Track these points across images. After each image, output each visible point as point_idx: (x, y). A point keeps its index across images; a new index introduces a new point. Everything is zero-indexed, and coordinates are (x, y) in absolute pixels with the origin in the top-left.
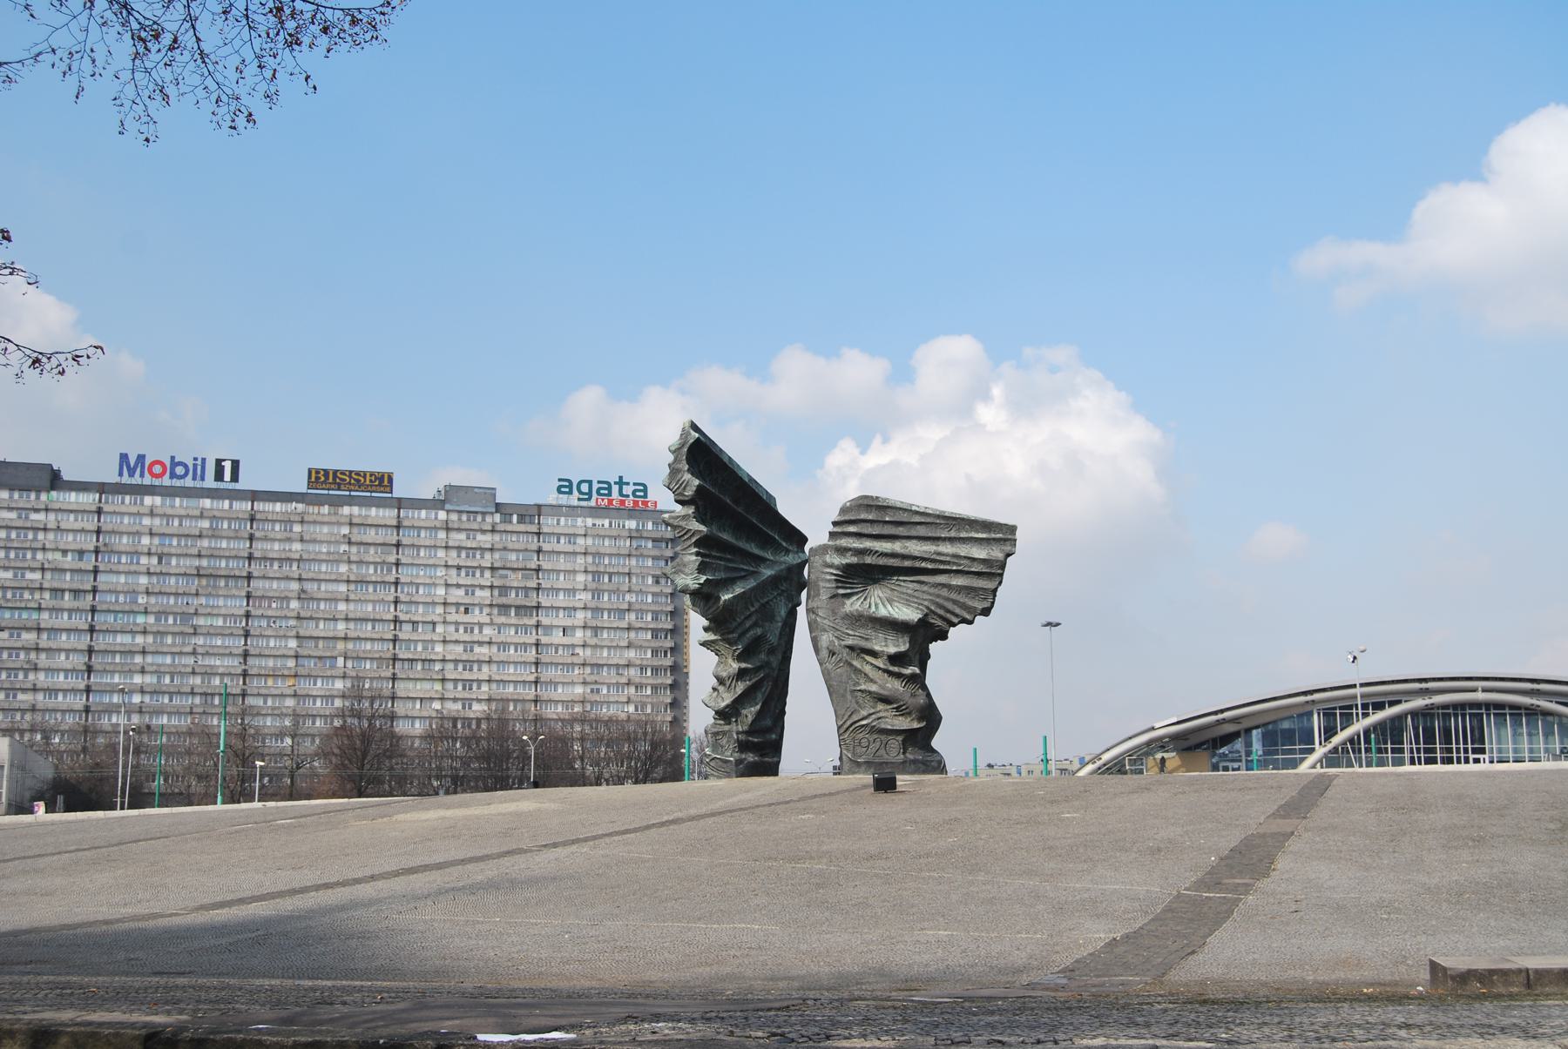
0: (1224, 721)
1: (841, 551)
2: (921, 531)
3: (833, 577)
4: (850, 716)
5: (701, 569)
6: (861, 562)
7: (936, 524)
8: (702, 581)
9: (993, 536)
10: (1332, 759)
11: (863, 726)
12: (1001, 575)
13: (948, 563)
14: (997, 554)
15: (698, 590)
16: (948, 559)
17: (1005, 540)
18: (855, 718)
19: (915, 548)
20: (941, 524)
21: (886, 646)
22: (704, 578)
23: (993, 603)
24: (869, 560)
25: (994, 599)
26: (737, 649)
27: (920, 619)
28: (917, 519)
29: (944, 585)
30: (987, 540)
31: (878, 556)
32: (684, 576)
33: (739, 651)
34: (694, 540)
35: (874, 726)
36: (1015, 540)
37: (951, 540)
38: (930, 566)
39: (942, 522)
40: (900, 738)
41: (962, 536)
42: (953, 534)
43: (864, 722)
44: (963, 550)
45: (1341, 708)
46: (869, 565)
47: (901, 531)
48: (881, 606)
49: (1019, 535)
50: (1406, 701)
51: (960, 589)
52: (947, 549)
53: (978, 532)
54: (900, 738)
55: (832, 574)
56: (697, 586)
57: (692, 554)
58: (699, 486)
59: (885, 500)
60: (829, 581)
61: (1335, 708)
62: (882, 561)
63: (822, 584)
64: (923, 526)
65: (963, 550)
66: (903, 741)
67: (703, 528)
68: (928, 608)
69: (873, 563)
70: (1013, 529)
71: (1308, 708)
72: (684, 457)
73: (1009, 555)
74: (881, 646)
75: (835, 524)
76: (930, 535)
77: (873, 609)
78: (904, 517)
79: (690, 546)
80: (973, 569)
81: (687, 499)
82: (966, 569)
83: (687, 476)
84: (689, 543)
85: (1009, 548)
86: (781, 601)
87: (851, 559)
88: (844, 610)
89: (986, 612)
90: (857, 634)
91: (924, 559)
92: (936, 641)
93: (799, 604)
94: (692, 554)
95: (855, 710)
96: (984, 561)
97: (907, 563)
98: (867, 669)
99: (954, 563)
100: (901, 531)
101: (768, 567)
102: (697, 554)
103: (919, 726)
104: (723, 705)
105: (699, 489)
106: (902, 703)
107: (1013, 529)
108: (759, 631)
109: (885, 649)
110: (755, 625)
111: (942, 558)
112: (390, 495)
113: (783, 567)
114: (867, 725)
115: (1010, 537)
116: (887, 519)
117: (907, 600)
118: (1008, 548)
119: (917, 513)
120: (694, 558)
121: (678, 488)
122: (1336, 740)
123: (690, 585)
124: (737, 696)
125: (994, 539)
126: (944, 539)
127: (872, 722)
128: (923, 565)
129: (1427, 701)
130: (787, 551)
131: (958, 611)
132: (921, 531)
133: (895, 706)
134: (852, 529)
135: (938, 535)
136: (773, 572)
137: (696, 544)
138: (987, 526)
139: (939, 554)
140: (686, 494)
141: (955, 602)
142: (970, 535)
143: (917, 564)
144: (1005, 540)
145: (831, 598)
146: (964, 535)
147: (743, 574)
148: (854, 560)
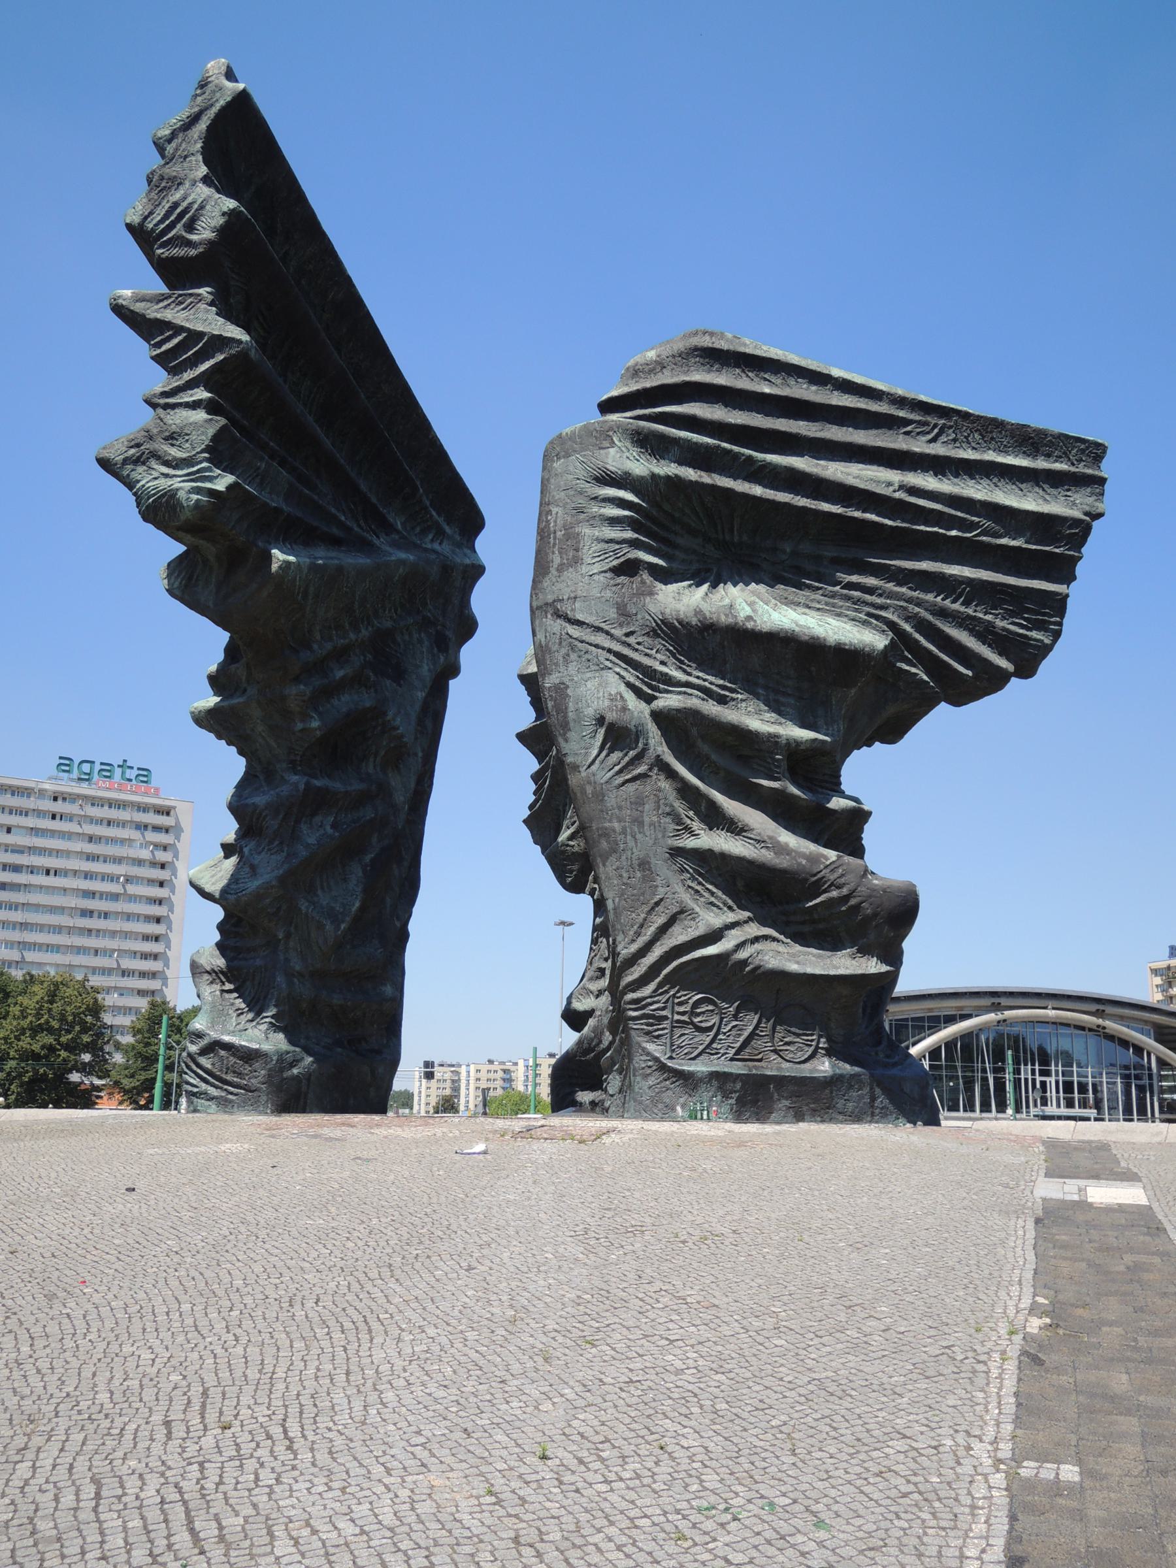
3: (627, 513)
4: (663, 930)
12: (1074, 561)
20: (910, 422)
22: (230, 479)
25: (1060, 624)
32: (165, 470)
35: (745, 962)
39: (912, 416)
42: (938, 449)
44: (977, 490)
50: (976, 1016)
55: (621, 503)
57: (194, 405)
58: (231, 214)
60: (613, 521)
61: (907, 1020)
63: (586, 531)
68: (892, 626)
70: (1096, 452)
72: (199, 145)
81: (193, 252)
84: (188, 375)
85: (1090, 500)
86: (420, 641)
87: (668, 469)
94: (194, 405)
95: (682, 912)
99: (952, 522)
101: (396, 545)
102: (212, 407)
105: (232, 225)
107: (1096, 452)
108: (367, 700)
110: (357, 681)
111: (922, 502)
115: (1081, 469)
117: (827, 604)
120: (201, 415)
123: (182, 495)
129: (1000, 1016)
130: (440, 534)
139: (914, 491)
140: (194, 237)
145: (617, 571)
147: (335, 531)
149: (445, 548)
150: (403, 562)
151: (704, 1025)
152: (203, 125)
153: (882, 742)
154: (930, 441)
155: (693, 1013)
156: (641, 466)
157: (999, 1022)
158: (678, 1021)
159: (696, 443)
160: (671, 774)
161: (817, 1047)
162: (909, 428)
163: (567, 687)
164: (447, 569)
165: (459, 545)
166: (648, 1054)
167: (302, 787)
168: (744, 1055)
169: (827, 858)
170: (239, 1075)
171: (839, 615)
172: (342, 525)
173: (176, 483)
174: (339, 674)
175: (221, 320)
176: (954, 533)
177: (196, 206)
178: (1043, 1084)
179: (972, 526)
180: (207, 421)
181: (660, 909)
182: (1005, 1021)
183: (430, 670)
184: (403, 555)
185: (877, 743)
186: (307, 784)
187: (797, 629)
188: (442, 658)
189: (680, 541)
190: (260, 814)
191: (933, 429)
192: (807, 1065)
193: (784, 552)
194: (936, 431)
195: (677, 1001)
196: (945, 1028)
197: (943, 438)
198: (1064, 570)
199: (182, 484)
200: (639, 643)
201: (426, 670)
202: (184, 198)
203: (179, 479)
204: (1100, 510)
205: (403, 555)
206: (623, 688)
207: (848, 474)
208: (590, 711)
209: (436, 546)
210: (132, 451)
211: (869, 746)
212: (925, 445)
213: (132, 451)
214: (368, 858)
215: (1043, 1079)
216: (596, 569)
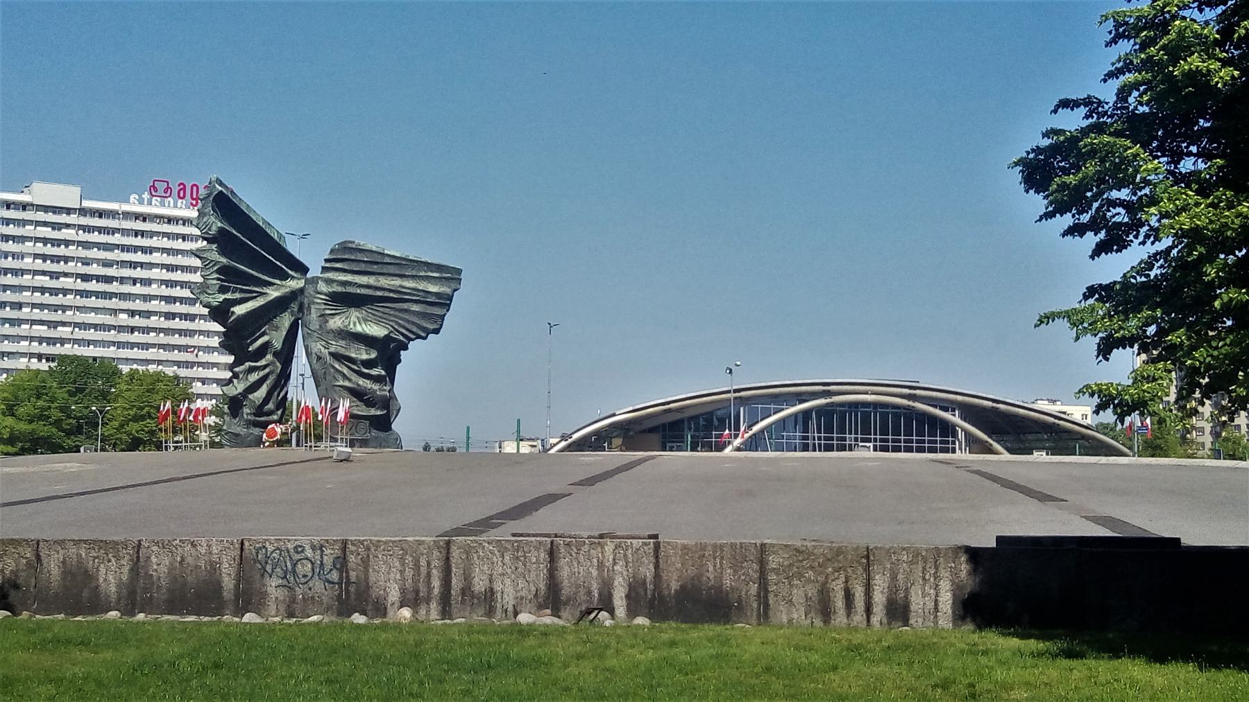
0: (670, 410)
1: (329, 282)
8: (221, 300)
10: (754, 444)
12: (449, 305)
14: (445, 289)
15: (216, 307)
16: (409, 291)
19: (384, 282)
23: (442, 325)
28: (387, 260)
34: (215, 268)
37: (413, 277)
41: (421, 274)
42: (414, 274)
44: (422, 286)
47: (375, 268)
48: (357, 324)
52: (410, 284)
53: (432, 272)
64: (392, 266)
65: (422, 286)
70: (459, 271)
73: (455, 290)
75: (327, 260)
76: (397, 272)
77: (352, 326)
81: (211, 236)
84: (212, 271)
85: (456, 285)
89: (437, 331)
91: (390, 291)
96: (437, 295)
97: (379, 293)
98: (345, 370)
99: (414, 295)
101: (276, 290)
103: (382, 413)
107: (459, 271)
109: (359, 356)
113: (288, 290)
115: (456, 276)
116: (366, 259)
118: (454, 286)
121: (205, 228)
122: (756, 428)
125: (445, 278)
128: (392, 295)
129: (829, 400)
130: (293, 278)
131: (415, 329)
132: (392, 270)
134: (338, 265)
137: (218, 271)
138: (439, 268)
141: (413, 323)
142: (427, 274)
143: (387, 294)
145: (320, 316)
147: (254, 295)
148: (340, 289)
160: (334, 367)
173: (210, 300)
179: (419, 296)
198: (447, 306)
206: (321, 347)
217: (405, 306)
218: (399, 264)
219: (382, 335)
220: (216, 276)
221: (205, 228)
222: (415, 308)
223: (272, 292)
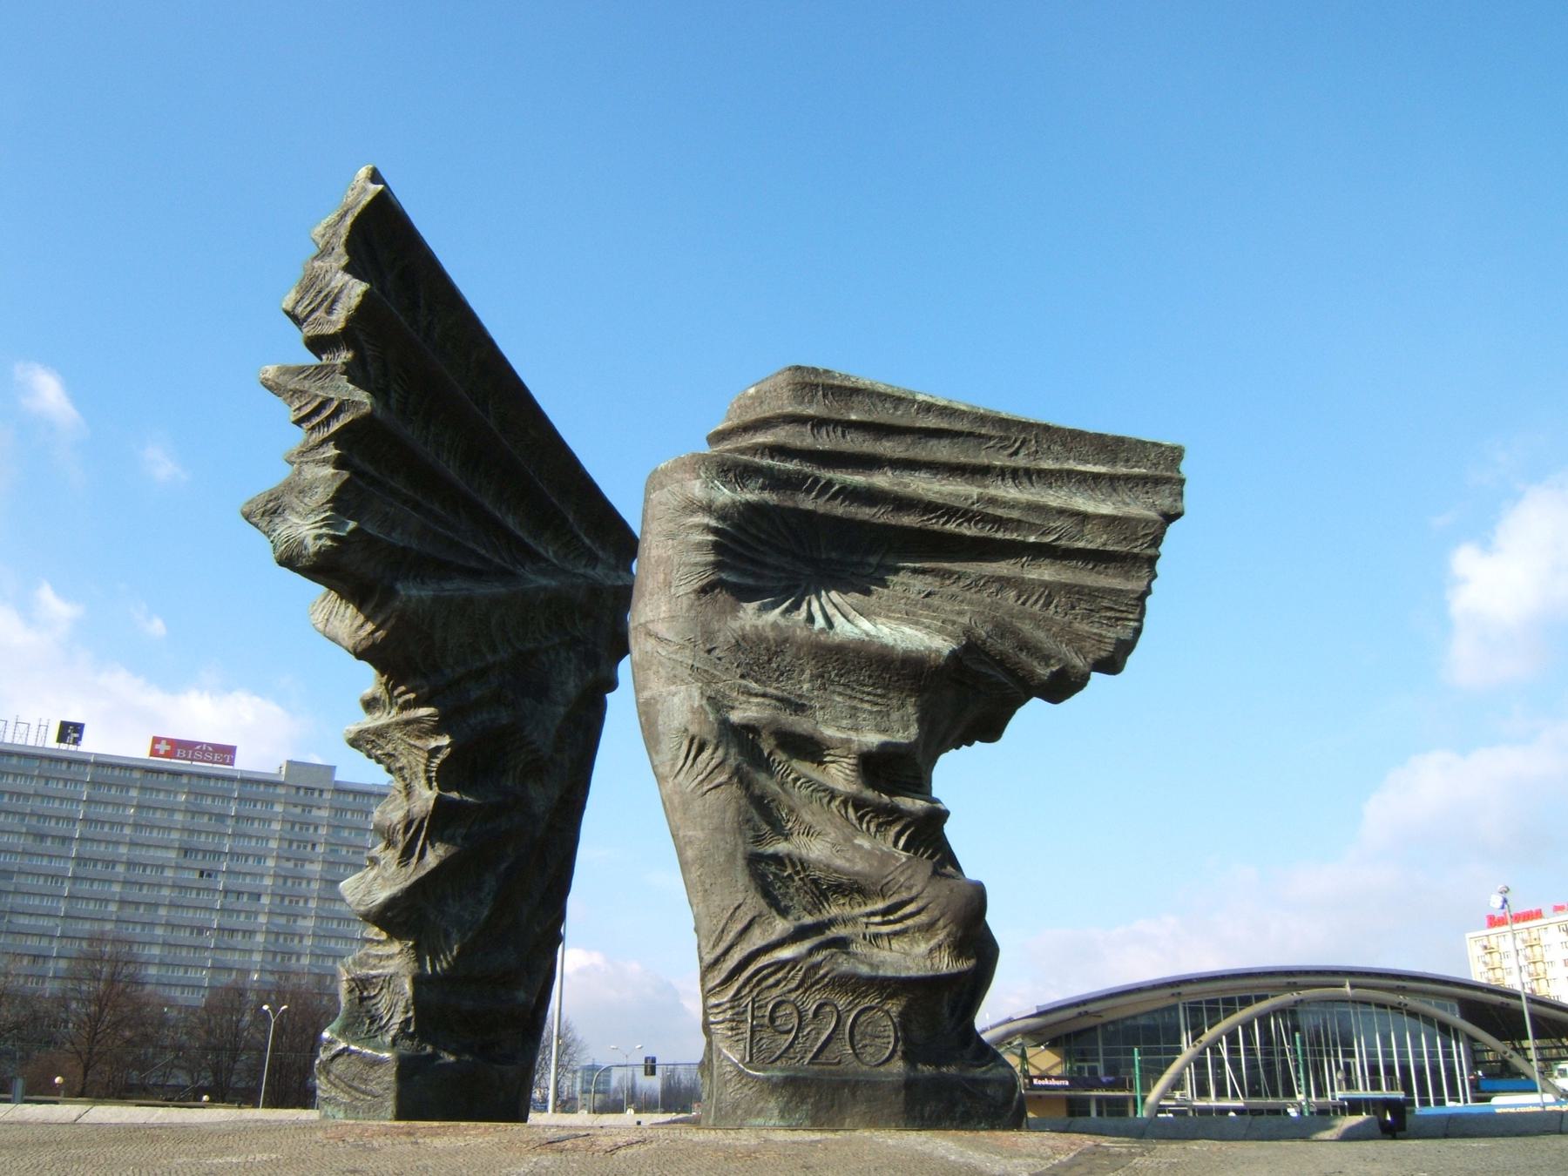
2: (942, 451)
5: (342, 503)
6: (790, 504)
7: (980, 436)
9: (1121, 469)
11: (781, 965)
12: (1152, 561)
13: (1018, 524)
14: (1137, 507)
16: (1015, 514)
17: (1157, 481)
18: (757, 939)
20: (990, 438)
21: (856, 729)
22: (352, 525)
23: (1138, 631)
24: (807, 502)
25: (1140, 620)
26: (438, 749)
27: (953, 652)
28: (931, 422)
29: (1004, 582)
30: (1113, 479)
31: (834, 497)
33: (441, 756)
34: (335, 426)
36: (1182, 482)
37: (1015, 474)
38: (969, 530)
40: (894, 1007)
42: (1021, 461)
43: (786, 953)
44: (1054, 498)
45: (1208, 1002)
46: (810, 514)
47: (888, 448)
49: (1185, 468)
50: (1272, 996)
51: (1050, 591)
54: (894, 1007)
56: (329, 543)
57: (325, 461)
59: (847, 377)
61: (1200, 1002)
62: (840, 509)
64: (945, 442)
66: (901, 1015)
67: (362, 396)
69: (821, 510)
70: (1175, 455)
71: (1172, 1001)
74: (839, 728)
76: (963, 459)
77: (820, 622)
78: (899, 417)
79: (324, 442)
80: (1081, 545)
82: (1063, 542)
83: (341, 279)
87: (751, 495)
88: (735, 625)
89: (1112, 665)
90: (770, 690)
91: (951, 512)
92: (969, 744)
93: (612, 685)
94: (325, 461)
97: (909, 520)
99: (1032, 528)
100: (888, 448)
102: (339, 463)
104: (382, 895)
106: (905, 895)
107: (1175, 455)
108: (505, 718)
111: (1000, 512)
112: (231, 767)
114: (793, 962)
116: (853, 417)
118: (1165, 502)
119: (928, 408)
120: (329, 471)
123: (309, 541)
124: (422, 873)
125: (1128, 478)
126: (1002, 473)
127: (811, 952)
130: (593, 560)
132: (942, 451)
133: (880, 905)
135: (983, 459)
136: (554, 583)
137: (338, 438)
139: (993, 501)
142: (1066, 466)
143: (936, 525)
144: (1157, 481)
146: (1048, 464)
147: (473, 564)
148: (770, 497)
149: (599, 573)
150: (545, 589)
151: (781, 1028)
152: (349, 220)
153: (983, 740)
154: (1011, 455)
155: (772, 1019)
156: (725, 495)
157: (1296, 1002)
158: (757, 1025)
159: (779, 470)
161: (894, 1051)
162: (992, 443)
163: (657, 702)
164: (596, 591)
165: (616, 568)
166: (729, 1059)
167: (431, 803)
168: (822, 1059)
169: (897, 859)
170: (365, 1081)
171: (917, 623)
172: (482, 559)
174: (475, 694)
175: (351, 387)
176: (1032, 539)
177: (336, 291)
178: (1347, 1066)
180: (333, 475)
181: (740, 913)
182: (1302, 1001)
183: (576, 686)
184: (544, 581)
185: (977, 743)
186: (439, 800)
187: (867, 639)
188: (590, 675)
189: (769, 560)
190: (394, 829)
191: (1015, 441)
192: (882, 1069)
193: (870, 565)
194: (1017, 445)
195: (756, 1005)
196: (1241, 1009)
197: (1023, 452)
199: (308, 532)
200: (720, 659)
201: (572, 686)
202: (327, 286)
203: (308, 527)
204: (1179, 510)
205: (544, 581)
207: (929, 490)
208: (676, 724)
209: (590, 572)
210: (271, 504)
211: (957, 748)
212: (1006, 458)
213: (271, 504)
214: (503, 867)
215: (1348, 1060)
216: (681, 591)
217: (1003, 568)
218: (970, 434)
219: (946, 652)
220: (331, 451)
221: (313, 311)
222: (1045, 572)
223: (531, 577)
